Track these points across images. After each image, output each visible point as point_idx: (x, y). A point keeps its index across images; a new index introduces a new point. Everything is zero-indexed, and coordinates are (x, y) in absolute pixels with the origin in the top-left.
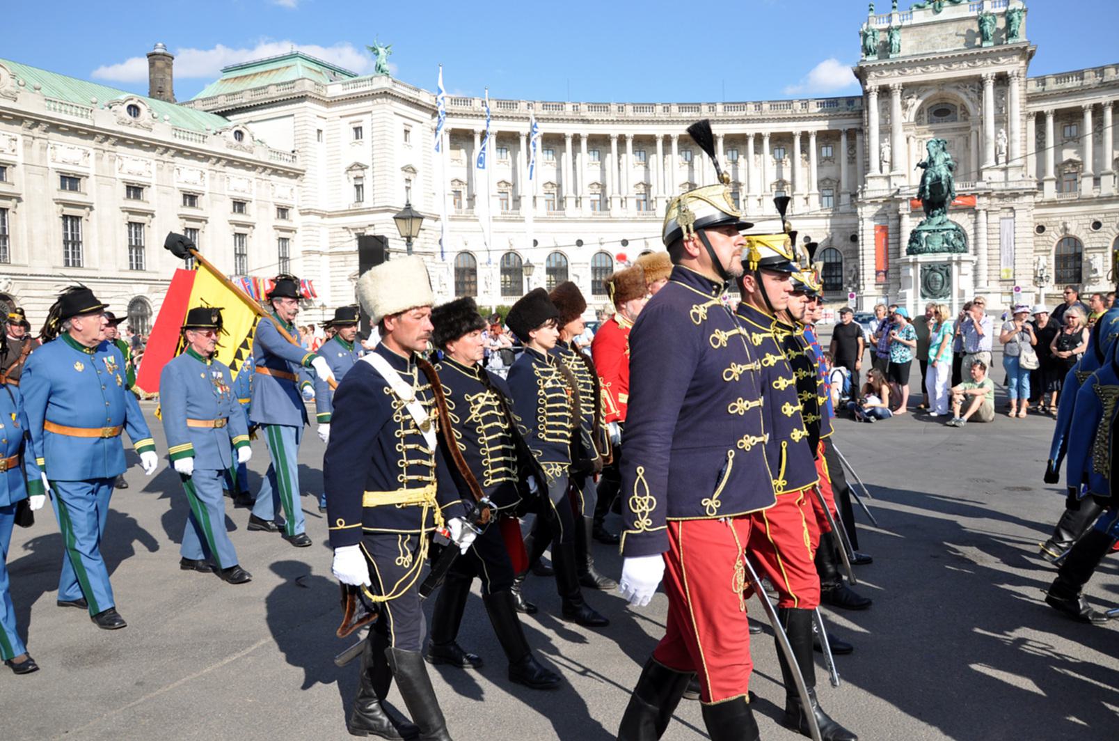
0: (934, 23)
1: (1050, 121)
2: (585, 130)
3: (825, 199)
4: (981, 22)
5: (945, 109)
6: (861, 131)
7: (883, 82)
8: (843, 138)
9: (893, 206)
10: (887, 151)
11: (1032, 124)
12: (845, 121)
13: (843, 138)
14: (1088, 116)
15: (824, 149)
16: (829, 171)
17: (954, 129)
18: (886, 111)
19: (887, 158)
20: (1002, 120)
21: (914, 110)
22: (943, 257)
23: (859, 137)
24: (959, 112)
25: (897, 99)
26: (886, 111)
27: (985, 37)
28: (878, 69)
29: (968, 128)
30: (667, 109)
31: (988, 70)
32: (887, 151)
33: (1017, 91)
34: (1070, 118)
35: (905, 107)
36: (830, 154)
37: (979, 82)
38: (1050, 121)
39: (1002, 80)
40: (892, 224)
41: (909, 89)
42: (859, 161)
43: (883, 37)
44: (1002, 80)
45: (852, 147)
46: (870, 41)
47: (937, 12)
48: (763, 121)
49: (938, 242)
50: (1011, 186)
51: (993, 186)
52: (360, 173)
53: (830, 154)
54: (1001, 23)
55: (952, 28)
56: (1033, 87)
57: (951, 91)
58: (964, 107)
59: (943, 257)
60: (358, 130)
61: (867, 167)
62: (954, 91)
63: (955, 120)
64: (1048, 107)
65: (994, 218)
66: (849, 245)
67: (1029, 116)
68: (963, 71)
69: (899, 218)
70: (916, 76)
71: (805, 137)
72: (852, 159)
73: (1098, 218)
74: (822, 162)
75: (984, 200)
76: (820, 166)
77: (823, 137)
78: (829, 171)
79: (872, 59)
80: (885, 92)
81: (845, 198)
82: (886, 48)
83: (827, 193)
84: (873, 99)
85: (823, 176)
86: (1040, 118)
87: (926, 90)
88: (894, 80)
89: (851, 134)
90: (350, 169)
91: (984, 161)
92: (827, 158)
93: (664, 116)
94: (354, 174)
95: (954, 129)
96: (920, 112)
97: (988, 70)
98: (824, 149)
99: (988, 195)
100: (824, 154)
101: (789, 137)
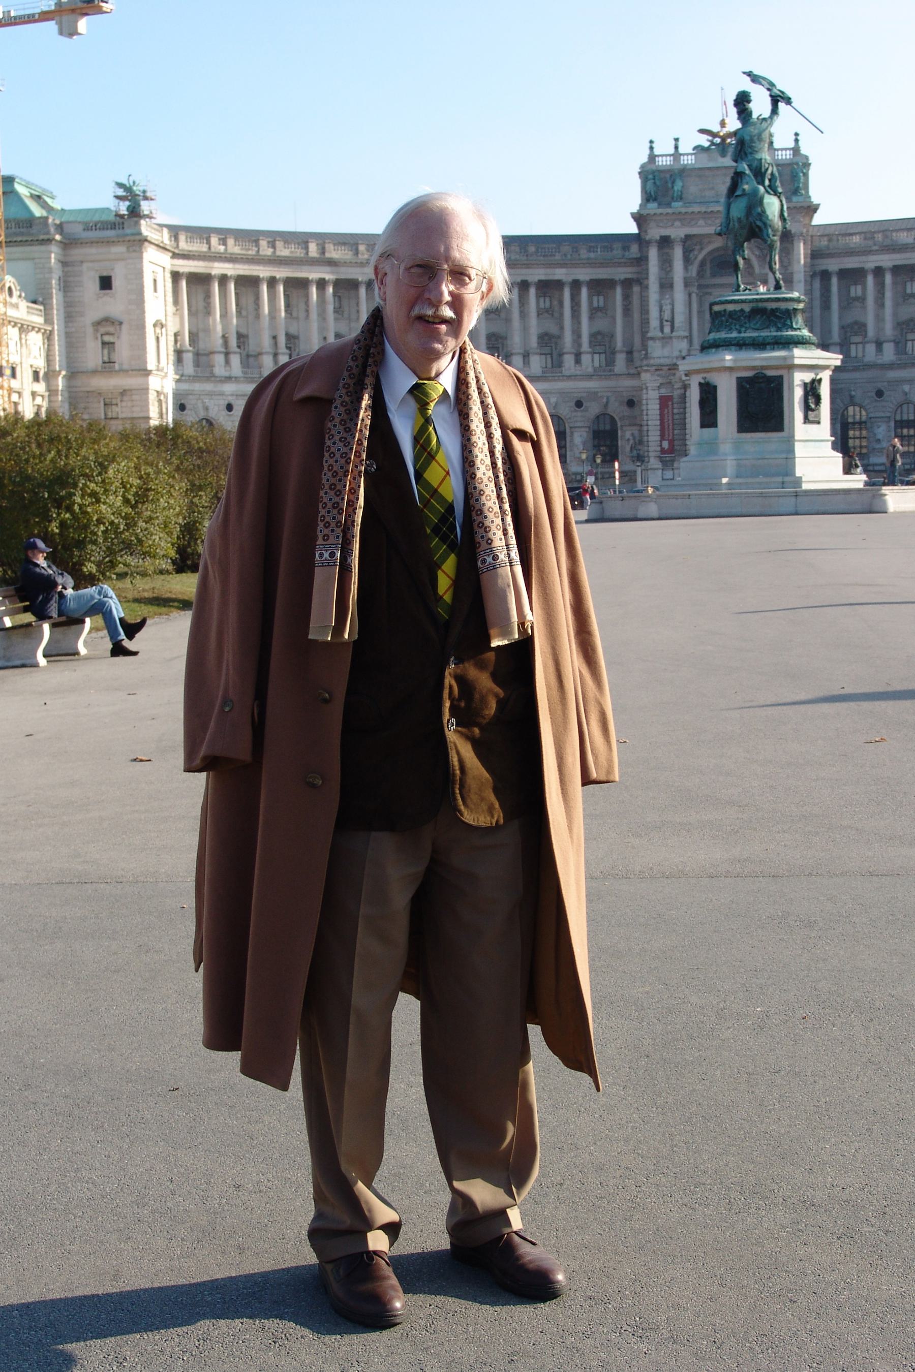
0: (718, 168)
1: (834, 280)
3: (596, 356)
8: (619, 290)
11: (817, 284)
12: (621, 270)
13: (619, 290)
14: (870, 279)
15: (595, 299)
16: (601, 324)
18: (666, 263)
19: (667, 315)
23: (636, 289)
26: (666, 263)
34: (852, 276)
35: (687, 261)
36: (601, 304)
40: (676, 393)
42: (636, 316)
45: (627, 297)
48: (528, 266)
52: (111, 329)
53: (601, 304)
60: (106, 283)
61: (645, 322)
64: (833, 265)
66: (626, 411)
69: (685, 387)
71: (576, 285)
72: (627, 311)
73: (879, 385)
74: (594, 312)
76: (591, 318)
78: (601, 324)
80: (665, 242)
81: (621, 359)
83: (598, 349)
84: (653, 254)
85: (595, 330)
87: (709, 242)
88: (677, 232)
89: (627, 284)
90: (98, 324)
92: (598, 309)
94: (102, 330)
96: (702, 264)
98: (595, 299)
100: (595, 304)
101: (559, 284)
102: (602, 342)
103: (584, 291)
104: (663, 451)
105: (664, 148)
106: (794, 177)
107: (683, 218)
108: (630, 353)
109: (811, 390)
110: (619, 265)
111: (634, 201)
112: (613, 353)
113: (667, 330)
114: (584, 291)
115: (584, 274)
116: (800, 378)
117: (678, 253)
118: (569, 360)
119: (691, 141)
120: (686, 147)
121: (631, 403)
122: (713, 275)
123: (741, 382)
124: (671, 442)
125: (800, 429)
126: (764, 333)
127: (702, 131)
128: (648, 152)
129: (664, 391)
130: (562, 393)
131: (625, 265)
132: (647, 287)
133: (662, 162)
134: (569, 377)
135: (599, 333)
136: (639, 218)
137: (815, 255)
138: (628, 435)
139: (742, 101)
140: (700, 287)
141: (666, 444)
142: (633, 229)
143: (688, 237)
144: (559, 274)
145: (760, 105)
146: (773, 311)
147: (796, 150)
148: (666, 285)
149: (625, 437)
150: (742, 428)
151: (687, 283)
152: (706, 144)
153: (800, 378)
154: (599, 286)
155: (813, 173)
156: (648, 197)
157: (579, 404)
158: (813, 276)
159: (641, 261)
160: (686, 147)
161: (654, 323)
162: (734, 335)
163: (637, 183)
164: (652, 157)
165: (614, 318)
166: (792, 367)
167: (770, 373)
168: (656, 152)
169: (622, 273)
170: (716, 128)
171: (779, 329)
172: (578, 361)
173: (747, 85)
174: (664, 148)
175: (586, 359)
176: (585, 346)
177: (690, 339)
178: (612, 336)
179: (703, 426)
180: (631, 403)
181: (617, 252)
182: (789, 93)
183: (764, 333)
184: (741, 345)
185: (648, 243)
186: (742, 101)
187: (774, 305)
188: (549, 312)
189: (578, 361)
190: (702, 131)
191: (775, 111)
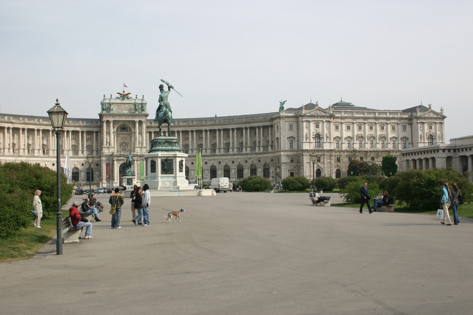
0: (122, 103)
1: (153, 134)
2: (11, 126)
4: (135, 105)
5: (125, 128)
6: (100, 132)
7: (108, 119)
8: (95, 134)
9: (111, 157)
10: (108, 139)
11: (148, 135)
13: (95, 134)
17: (127, 134)
20: (141, 133)
21: (116, 128)
22: (131, 177)
23: (99, 134)
24: (129, 129)
25: (112, 125)
27: (136, 110)
28: (106, 115)
29: (131, 134)
30: (39, 121)
31: (137, 119)
32: (108, 139)
33: (144, 126)
35: (114, 127)
37: (134, 123)
38: (153, 134)
39: (140, 122)
40: (111, 163)
41: (115, 122)
42: (99, 141)
43: (107, 106)
44: (140, 122)
45: (97, 136)
46: (104, 107)
47: (123, 100)
49: (130, 174)
50: (143, 154)
51: (138, 154)
54: (140, 106)
55: (127, 105)
56: (149, 124)
57: (126, 123)
58: (130, 128)
59: (131, 177)
61: (102, 143)
62: (127, 123)
63: (127, 131)
64: (152, 130)
65: (139, 162)
66: (96, 167)
67: (147, 132)
68: (131, 119)
69: (113, 161)
70: (117, 119)
72: (97, 140)
74: (87, 139)
75: (136, 158)
77: (88, 133)
78: (89, 143)
79: (104, 112)
80: (108, 122)
81: (95, 153)
82: (109, 109)
84: (105, 125)
86: (150, 133)
88: (111, 119)
89: (97, 132)
91: (136, 145)
93: (38, 123)
95: (127, 134)
96: (118, 128)
97: (137, 119)
99: (137, 156)
101: (78, 132)
102: (90, 148)
103: (85, 134)
104: (107, 178)
105: (108, 97)
106: (142, 107)
107: (113, 115)
108: (97, 151)
109: (181, 163)
110: (95, 127)
111: (100, 111)
112: (93, 151)
113: (108, 145)
114: (85, 134)
115: (85, 130)
116: (178, 160)
117: (112, 125)
118: (80, 152)
119: (115, 95)
120: (114, 97)
121: (97, 165)
122: (120, 131)
123: (162, 160)
124: (109, 176)
125: (178, 173)
126: (168, 148)
127: (118, 93)
128: (103, 98)
129: (107, 162)
130: (78, 161)
131: (96, 127)
132: (103, 134)
133: (107, 101)
134: (80, 158)
135: (89, 145)
136: (101, 115)
137: (148, 127)
138: (96, 174)
139: (161, 87)
140: (117, 134)
141: (108, 176)
142: (98, 118)
143: (114, 121)
144: (78, 129)
145: (166, 88)
146: (170, 142)
147: (142, 100)
148: (108, 133)
149: (96, 174)
150: (162, 173)
151: (114, 133)
152: (119, 97)
153: (178, 160)
154: (89, 133)
155: (147, 105)
156: (103, 110)
157: (83, 165)
158: (147, 132)
159: (101, 127)
160: (114, 97)
161: (105, 143)
162: (160, 148)
163: (100, 106)
164: (104, 99)
165: (93, 142)
166: (175, 157)
167: (170, 158)
168: (106, 98)
169: (95, 130)
170: (122, 93)
171: (172, 147)
172: (83, 153)
173: (162, 83)
174: (108, 97)
175: (85, 152)
176: (85, 149)
177: (114, 147)
178: (92, 147)
179: (152, 172)
180: (97, 165)
181: (94, 124)
182: (173, 86)
183: (168, 148)
184: (162, 150)
185: (103, 122)
186: (161, 87)
187: (171, 141)
188: (76, 139)
189: (83, 153)
190: (118, 93)
191: (169, 90)
